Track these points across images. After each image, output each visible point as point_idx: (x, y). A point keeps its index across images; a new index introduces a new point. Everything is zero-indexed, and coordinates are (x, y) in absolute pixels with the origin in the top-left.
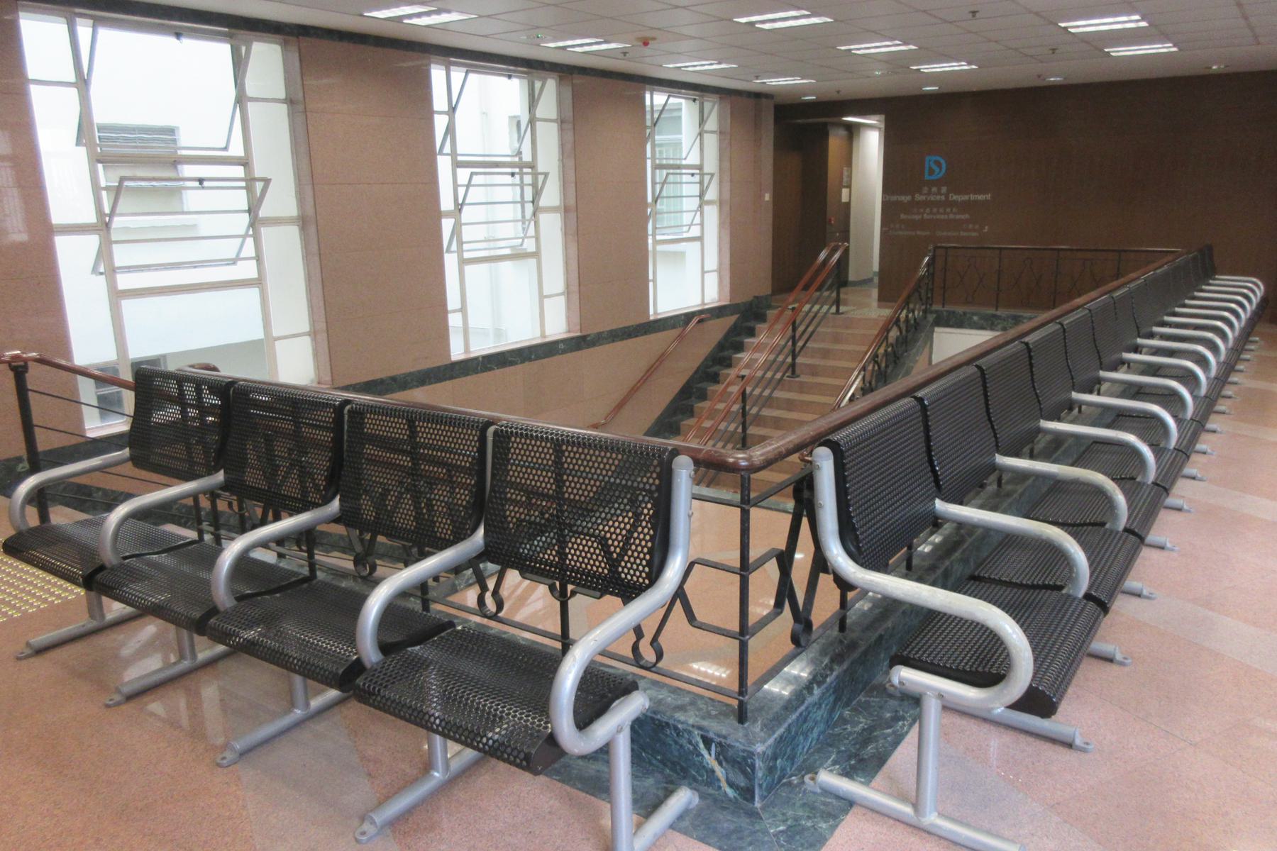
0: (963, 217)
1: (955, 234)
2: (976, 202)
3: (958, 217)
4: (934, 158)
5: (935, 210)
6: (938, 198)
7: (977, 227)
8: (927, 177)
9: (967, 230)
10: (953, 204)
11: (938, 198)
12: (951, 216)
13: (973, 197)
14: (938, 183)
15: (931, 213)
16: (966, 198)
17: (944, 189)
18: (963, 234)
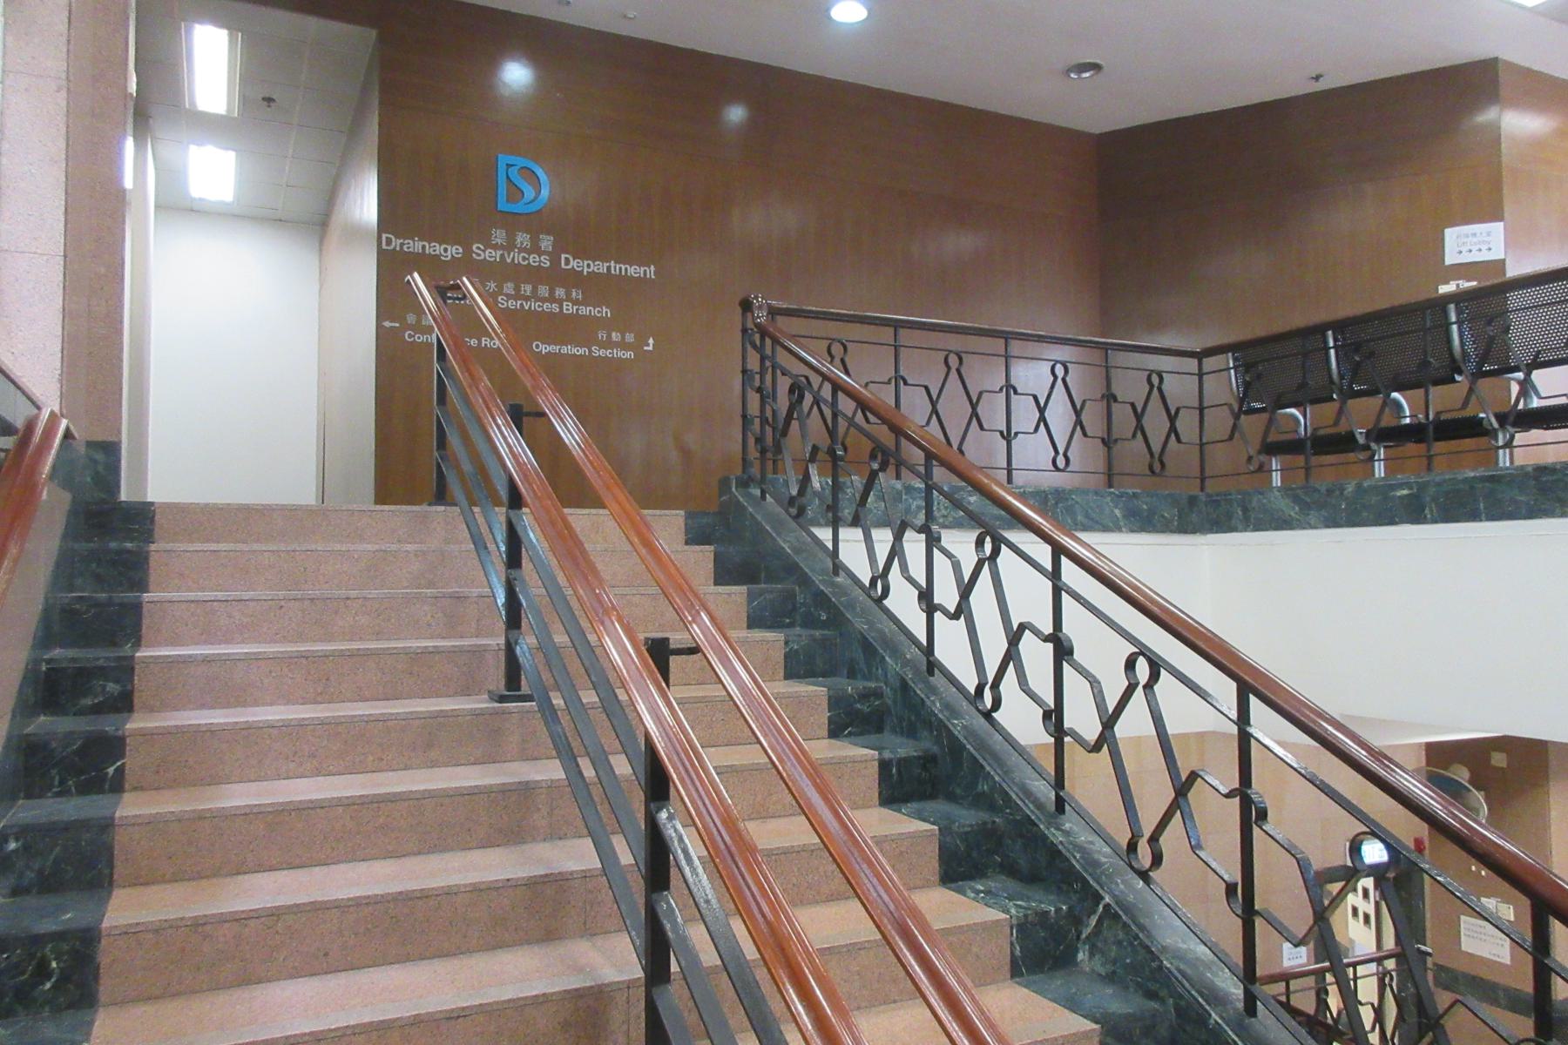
0: (595, 312)
1: (581, 351)
2: (623, 279)
3: (585, 311)
4: (521, 162)
5: (527, 289)
6: (533, 259)
7: (630, 338)
8: (503, 205)
9: (609, 344)
10: (574, 280)
11: (533, 259)
12: (568, 308)
13: (616, 268)
14: (535, 223)
15: (517, 296)
16: (600, 267)
17: (546, 242)
18: (598, 352)
